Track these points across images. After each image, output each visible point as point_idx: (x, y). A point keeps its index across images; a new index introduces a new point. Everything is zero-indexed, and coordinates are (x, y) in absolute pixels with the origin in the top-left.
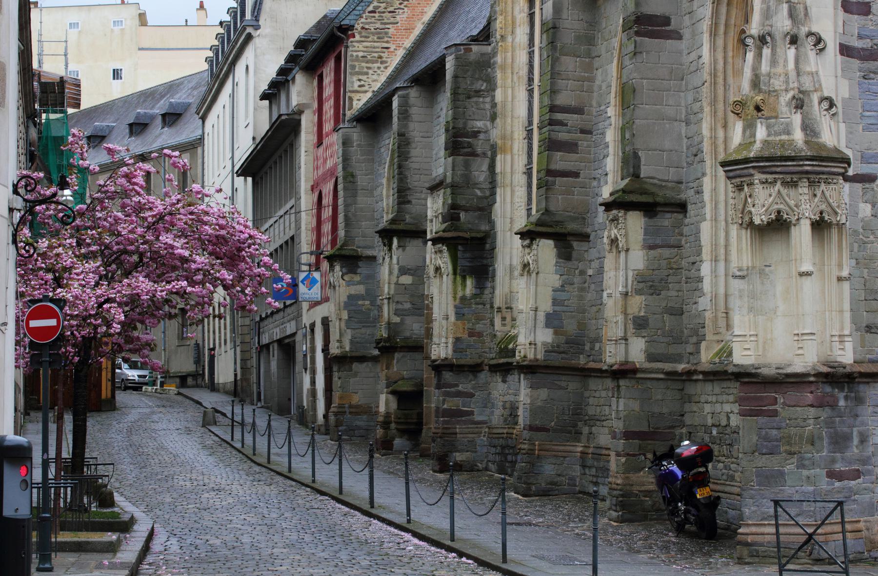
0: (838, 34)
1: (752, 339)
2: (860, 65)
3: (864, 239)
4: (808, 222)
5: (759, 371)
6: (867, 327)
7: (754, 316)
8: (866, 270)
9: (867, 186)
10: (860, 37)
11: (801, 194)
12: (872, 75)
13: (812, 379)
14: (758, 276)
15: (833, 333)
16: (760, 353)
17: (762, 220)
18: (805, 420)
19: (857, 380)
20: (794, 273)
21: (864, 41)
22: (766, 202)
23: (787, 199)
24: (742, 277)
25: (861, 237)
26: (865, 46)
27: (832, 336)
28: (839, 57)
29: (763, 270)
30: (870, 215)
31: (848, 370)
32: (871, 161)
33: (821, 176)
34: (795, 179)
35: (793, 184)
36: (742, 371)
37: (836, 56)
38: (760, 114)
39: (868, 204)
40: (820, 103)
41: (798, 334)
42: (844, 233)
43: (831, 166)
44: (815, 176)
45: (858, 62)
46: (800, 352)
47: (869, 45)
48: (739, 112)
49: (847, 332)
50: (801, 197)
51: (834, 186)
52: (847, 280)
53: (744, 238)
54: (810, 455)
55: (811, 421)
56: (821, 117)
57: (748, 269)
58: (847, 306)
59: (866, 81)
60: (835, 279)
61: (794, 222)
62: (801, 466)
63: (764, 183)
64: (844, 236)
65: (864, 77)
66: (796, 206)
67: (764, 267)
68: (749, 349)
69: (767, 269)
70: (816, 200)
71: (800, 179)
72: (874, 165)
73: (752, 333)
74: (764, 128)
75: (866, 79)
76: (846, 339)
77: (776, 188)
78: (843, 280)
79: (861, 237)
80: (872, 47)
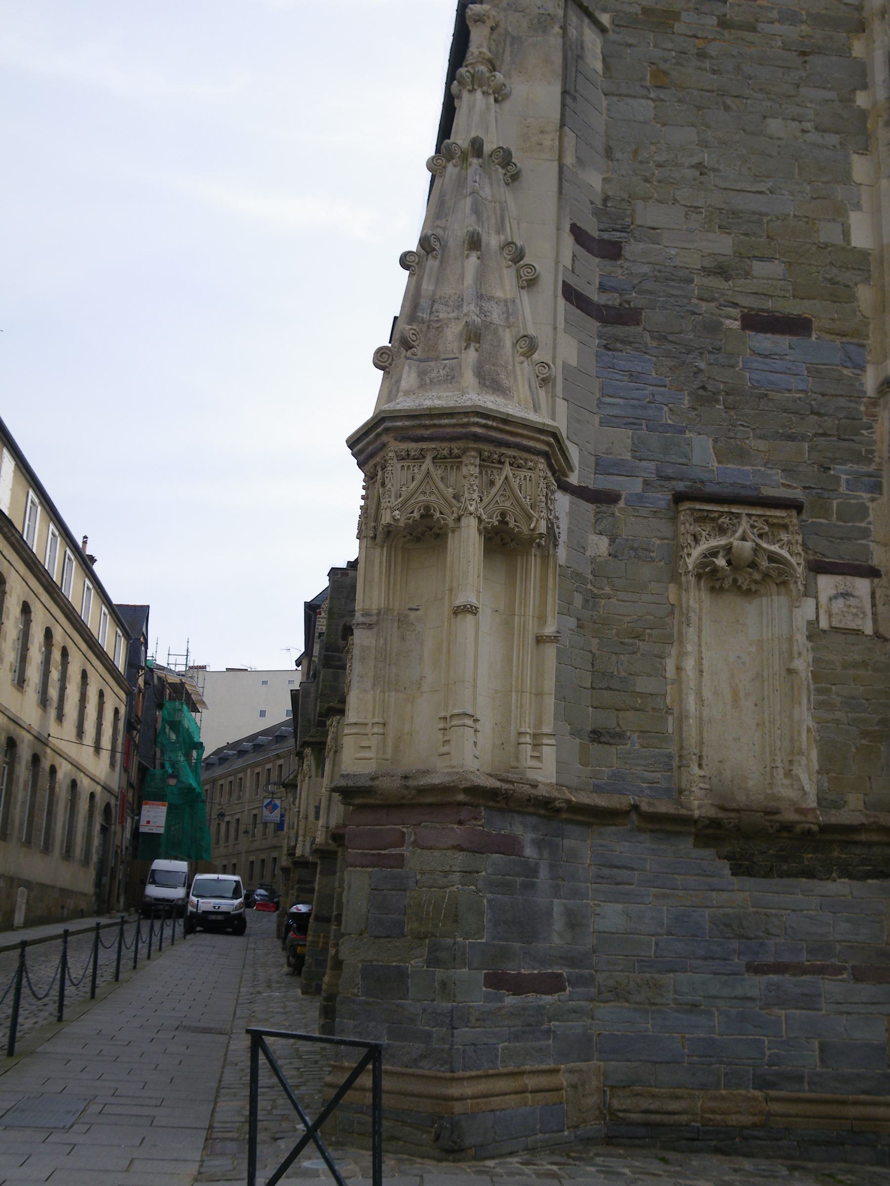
0: (561, 269)
1: (375, 730)
2: (600, 329)
3: (596, 591)
4: (474, 522)
5: (377, 783)
6: (594, 732)
7: (383, 692)
8: (597, 641)
9: (604, 508)
10: (602, 288)
11: (465, 477)
12: (619, 345)
13: (461, 797)
14: (396, 624)
15: (523, 730)
16: (389, 756)
17: (393, 518)
18: (446, 874)
19: (564, 816)
20: (447, 611)
22: (404, 489)
23: (441, 485)
24: (370, 626)
25: (589, 586)
26: (610, 303)
27: (520, 734)
28: (561, 302)
29: (406, 616)
30: (606, 554)
31: (542, 791)
32: (611, 471)
33: (504, 450)
34: (456, 451)
35: (452, 461)
36: (351, 784)
37: (555, 297)
38: (409, 353)
39: (603, 537)
40: (514, 345)
41: (446, 718)
42: (551, 564)
43: (522, 436)
44: (491, 448)
45: (599, 324)
46: (445, 749)
48: (387, 364)
49: (547, 729)
50: (466, 483)
51: (529, 474)
52: (552, 641)
53: (377, 562)
54: (449, 941)
55: (456, 877)
56: (514, 365)
57: (379, 614)
58: (550, 685)
59: (610, 353)
60: (530, 639)
61: (451, 524)
62: (434, 961)
63: (403, 459)
64: (551, 570)
65: (606, 347)
66: (456, 497)
67: (408, 612)
68: (370, 747)
69: (413, 614)
70: (494, 490)
71: (465, 451)
72: (615, 477)
73: (376, 720)
74: (414, 375)
75: (609, 349)
76: (545, 741)
77: (424, 467)
78: (545, 642)
79: (589, 586)
80: (621, 305)
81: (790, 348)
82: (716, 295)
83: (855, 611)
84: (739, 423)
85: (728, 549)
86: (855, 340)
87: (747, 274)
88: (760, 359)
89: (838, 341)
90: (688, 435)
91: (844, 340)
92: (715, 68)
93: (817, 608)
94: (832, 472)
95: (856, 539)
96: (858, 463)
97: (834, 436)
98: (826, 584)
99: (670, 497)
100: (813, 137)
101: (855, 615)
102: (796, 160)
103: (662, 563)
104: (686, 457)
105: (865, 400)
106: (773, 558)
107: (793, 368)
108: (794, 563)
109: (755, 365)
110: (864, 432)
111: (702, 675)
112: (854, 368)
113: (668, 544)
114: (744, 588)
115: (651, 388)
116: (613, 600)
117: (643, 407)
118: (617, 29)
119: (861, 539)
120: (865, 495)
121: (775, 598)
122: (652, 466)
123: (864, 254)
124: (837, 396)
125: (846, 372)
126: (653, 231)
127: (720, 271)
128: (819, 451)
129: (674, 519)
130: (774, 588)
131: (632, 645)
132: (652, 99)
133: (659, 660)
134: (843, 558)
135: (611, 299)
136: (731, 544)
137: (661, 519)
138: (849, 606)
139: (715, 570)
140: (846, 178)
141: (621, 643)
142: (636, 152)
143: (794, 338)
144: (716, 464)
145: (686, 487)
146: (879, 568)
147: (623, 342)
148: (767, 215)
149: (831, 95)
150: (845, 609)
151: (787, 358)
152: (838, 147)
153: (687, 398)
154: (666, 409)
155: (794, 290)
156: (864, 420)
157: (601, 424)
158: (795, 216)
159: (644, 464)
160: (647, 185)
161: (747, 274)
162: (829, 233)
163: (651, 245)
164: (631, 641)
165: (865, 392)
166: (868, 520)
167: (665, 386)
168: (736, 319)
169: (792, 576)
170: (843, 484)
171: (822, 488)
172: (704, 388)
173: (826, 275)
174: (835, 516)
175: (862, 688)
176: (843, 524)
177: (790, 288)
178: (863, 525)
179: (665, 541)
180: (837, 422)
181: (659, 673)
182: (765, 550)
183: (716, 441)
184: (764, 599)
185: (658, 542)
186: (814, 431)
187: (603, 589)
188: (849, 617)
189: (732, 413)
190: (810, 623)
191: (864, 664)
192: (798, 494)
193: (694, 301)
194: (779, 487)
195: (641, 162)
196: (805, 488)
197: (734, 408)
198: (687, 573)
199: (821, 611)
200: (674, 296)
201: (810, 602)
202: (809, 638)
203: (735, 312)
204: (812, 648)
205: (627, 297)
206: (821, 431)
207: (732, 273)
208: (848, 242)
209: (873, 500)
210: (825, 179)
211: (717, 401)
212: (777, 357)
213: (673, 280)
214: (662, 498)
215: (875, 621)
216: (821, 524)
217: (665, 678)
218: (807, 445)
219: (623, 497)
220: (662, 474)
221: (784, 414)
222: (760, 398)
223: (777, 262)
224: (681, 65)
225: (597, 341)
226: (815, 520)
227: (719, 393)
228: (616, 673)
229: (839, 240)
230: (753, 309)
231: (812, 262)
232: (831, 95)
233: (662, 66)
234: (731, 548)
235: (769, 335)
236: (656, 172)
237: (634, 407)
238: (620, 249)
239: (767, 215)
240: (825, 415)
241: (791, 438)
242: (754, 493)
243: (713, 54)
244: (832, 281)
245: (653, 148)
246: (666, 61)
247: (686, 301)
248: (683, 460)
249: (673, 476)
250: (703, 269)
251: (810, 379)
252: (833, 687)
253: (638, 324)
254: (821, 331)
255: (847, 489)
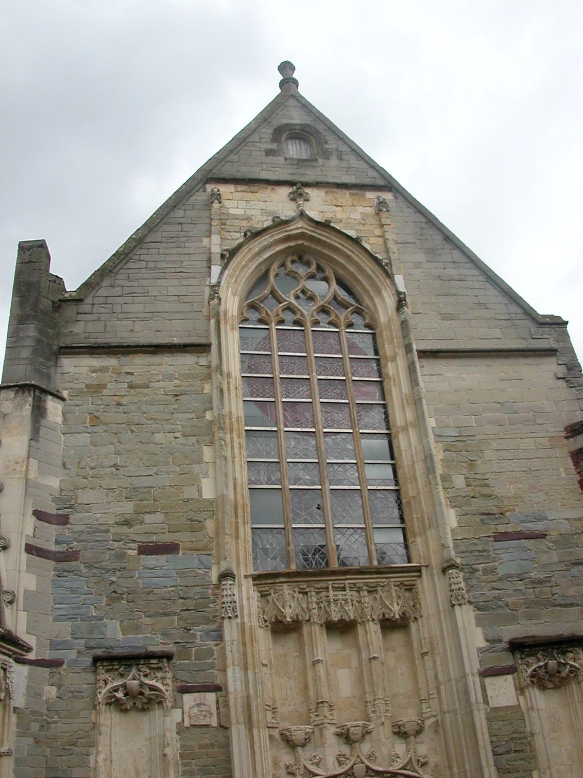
3: (49, 720)
8: (49, 749)
9: (55, 670)
10: (57, 542)
12: (66, 574)
21: (61, 546)
25: (45, 717)
26: (61, 550)
30: (55, 697)
32: (58, 648)
39: (53, 687)
47: (65, 549)
59: (59, 579)
72: (61, 651)
75: (60, 577)
79: (45, 717)
80: (67, 550)
81: (167, 562)
82: (123, 537)
83: (204, 713)
84: (136, 610)
85: (124, 686)
86: (205, 552)
87: (142, 522)
88: (148, 571)
89: (195, 553)
90: (105, 621)
91: (199, 552)
92: (125, 411)
93: (183, 714)
94: (192, 632)
95: (206, 670)
96: (207, 624)
97: (193, 610)
98: (189, 699)
99: (91, 659)
100: (182, 440)
101: (205, 716)
102: (171, 454)
103: (88, 699)
104: (103, 634)
105: (211, 586)
106: (152, 688)
107: (168, 573)
108: (164, 690)
109: (144, 575)
110: (211, 605)
111: (111, 763)
112: (204, 568)
113: (92, 687)
114: (140, 707)
115: (84, 596)
116: (60, 724)
117: (78, 608)
118: (72, 398)
119: (209, 669)
120: (212, 643)
121: (157, 711)
122: (82, 642)
123: (210, 502)
124: (195, 586)
125: (199, 571)
126: (87, 506)
127: (125, 523)
128: (184, 620)
129: (95, 672)
130: (156, 706)
131: (70, 749)
132: (89, 433)
133: (86, 756)
134: (198, 683)
135: (62, 548)
136: (125, 683)
137: (88, 672)
138: (201, 711)
139: (118, 700)
140: (199, 461)
141: (64, 749)
142: (79, 463)
143: (169, 556)
144: (122, 636)
145: (102, 652)
146: (221, 685)
147: (68, 571)
148: (154, 487)
149: (193, 415)
150: (198, 713)
151: (164, 568)
152: (196, 443)
153: (105, 599)
154: (92, 607)
155: (169, 528)
156: (211, 598)
157: (54, 620)
158: (170, 486)
159: (78, 641)
160: (85, 480)
161: (142, 522)
162: (190, 492)
163: (86, 514)
164: (70, 747)
165: (212, 582)
166: (214, 657)
167: (92, 594)
168: (134, 550)
169: (164, 698)
170: (198, 637)
171: (185, 642)
172: (115, 592)
173: (188, 517)
174: (193, 657)
175: (211, 759)
176: (198, 662)
177: (167, 527)
178: (211, 661)
179: (91, 685)
180: (195, 601)
181: (86, 765)
182: (146, 684)
183: (122, 622)
184: (152, 713)
185: (86, 686)
186: (181, 609)
187: (53, 718)
188: (202, 718)
189: (131, 604)
190: (178, 724)
191: (212, 745)
192: (171, 648)
193: (111, 542)
194: (159, 645)
195: (82, 468)
196: (175, 643)
197: (132, 602)
198: (99, 703)
199: (186, 716)
200: (99, 541)
201: (179, 711)
202: (178, 733)
203: (135, 546)
204: (180, 739)
205: (71, 545)
206: (185, 608)
207: (133, 523)
208: (201, 496)
209: (217, 645)
210: (187, 463)
211: (123, 599)
212: (158, 568)
213: (98, 532)
214: (88, 660)
215: (219, 718)
216: (185, 664)
217: (89, 767)
218: (176, 617)
219: (66, 662)
220: (88, 646)
221: (163, 601)
222: (148, 594)
223: (159, 513)
224: (106, 412)
225: (53, 573)
226: (182, 662)
227: (123, 594)
228: (60, 768)
229: (196, 495)
230: (145, 542)
231: (179, 511)
232: (193, 415)
233: (96, 414)
234: (126, 686)
235: (154, 556)
236: (90, 472)
237: (73, 608)
238: (68, 518)
239: (154, 487)
240: (188, 598)
241: (166, 615)
242: (143, 651)
243: (125, 403)
244: (191, 520)
245: (89, 459)
246: (98, 411)
247: (106, 543)
248: (102, 636)
249: (94, 646)
250: (116, 523)
251: (179, 578)
252: (193, 761)
253: (77, 560)
254: (184, 549)
255: (201, 641)
